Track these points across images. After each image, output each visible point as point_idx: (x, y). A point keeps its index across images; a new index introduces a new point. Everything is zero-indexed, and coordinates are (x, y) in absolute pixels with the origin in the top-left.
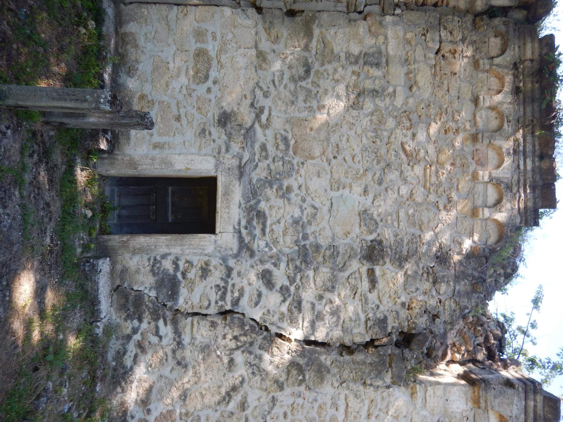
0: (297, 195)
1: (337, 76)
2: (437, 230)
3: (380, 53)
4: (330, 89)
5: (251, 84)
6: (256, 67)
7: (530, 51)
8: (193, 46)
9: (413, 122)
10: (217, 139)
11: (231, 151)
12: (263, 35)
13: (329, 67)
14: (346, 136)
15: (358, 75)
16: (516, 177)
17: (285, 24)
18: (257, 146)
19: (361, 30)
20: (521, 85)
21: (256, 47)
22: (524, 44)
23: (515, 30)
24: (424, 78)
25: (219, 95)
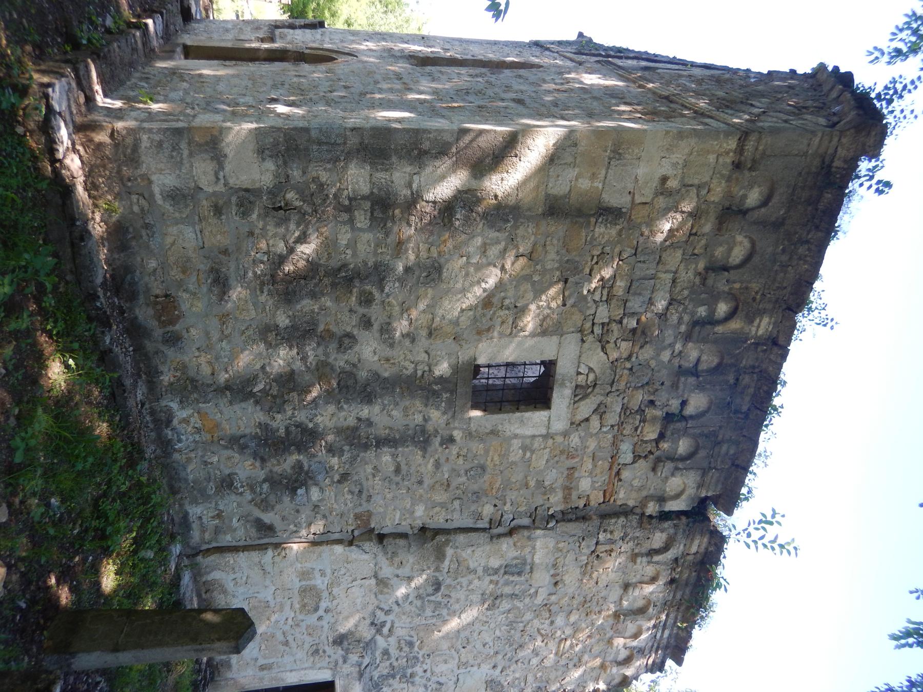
0: (422, 677)
1: (470, 588)
2: (563, 683)
3: (524, 563)
4: (463, 597)
5: (371, 608)
6: (375, 594)
7: (698, 545)
8: (297, 584)
9: (553, 611)
10: (332, 655)
11: (349, 661)
12: (383, 561)
13: (465, 581)
14: (477, 631)
15: (497, 583)
16: (650, 644)
17: (412, 550)
18: (378, 654)
19: (504, 547)
20: (677, 576)
21: (376, 576)
22: (692, 540)
23: (684, 531)
24: (571, 577)
25: (333, 620)
